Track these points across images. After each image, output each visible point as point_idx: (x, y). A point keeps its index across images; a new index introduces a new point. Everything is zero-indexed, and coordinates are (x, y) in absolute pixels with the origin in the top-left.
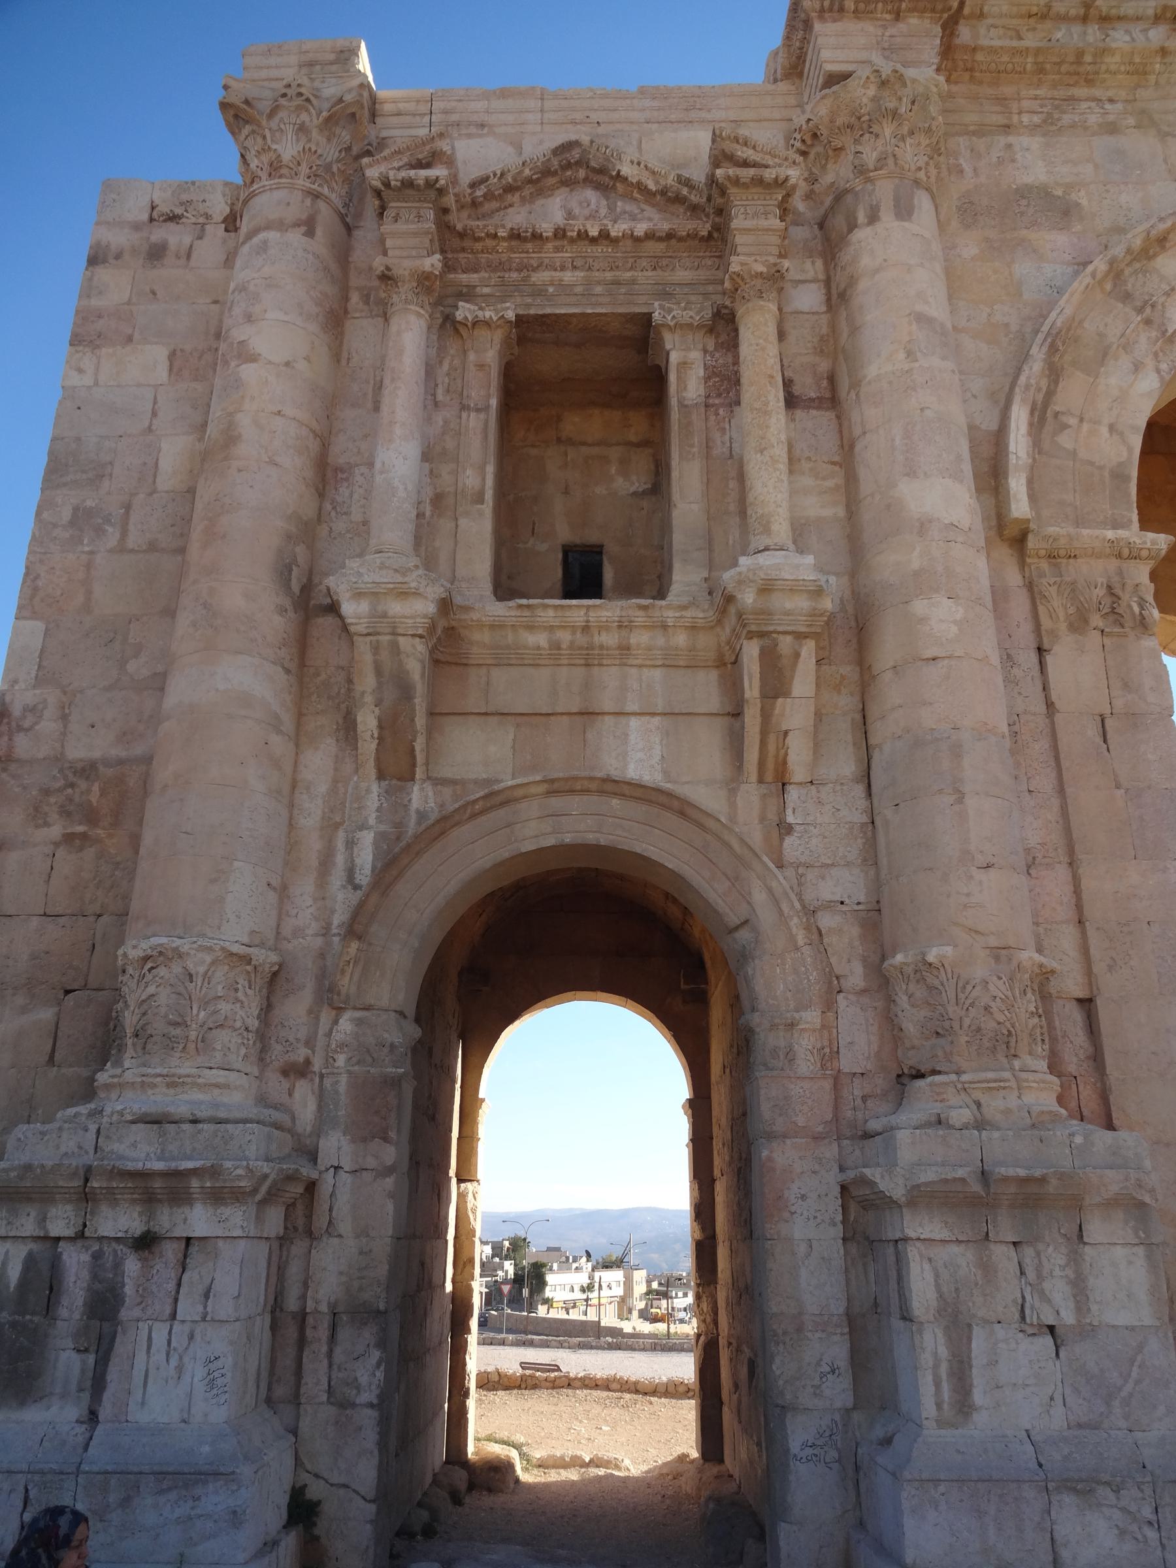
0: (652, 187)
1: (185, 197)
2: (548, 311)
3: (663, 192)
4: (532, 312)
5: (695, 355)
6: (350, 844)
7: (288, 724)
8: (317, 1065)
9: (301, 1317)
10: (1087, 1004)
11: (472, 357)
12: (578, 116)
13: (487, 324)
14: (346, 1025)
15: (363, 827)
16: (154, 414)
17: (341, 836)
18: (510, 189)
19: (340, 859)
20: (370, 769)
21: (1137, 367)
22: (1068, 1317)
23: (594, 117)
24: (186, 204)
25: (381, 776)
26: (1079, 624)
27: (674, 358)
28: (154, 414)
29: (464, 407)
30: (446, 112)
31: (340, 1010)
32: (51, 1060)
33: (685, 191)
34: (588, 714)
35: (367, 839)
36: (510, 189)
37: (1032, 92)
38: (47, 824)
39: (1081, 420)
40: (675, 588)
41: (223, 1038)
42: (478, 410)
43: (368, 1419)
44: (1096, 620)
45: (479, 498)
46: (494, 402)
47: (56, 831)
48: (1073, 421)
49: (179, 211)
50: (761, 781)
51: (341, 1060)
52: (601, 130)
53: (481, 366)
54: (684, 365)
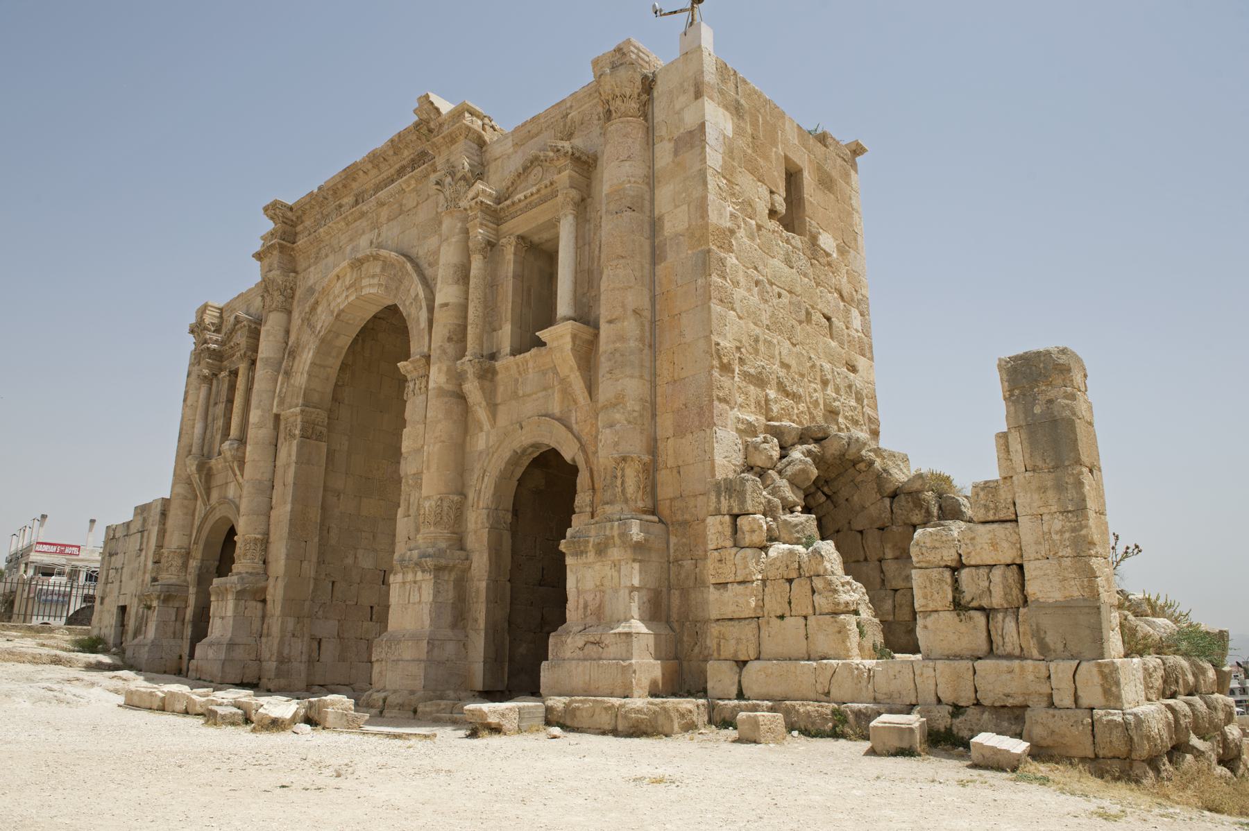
7: (190, 496)
18: (231, 333)
21: (309, 349)
34: (227, 483)
41: (173, 569)
43: (189, 641)
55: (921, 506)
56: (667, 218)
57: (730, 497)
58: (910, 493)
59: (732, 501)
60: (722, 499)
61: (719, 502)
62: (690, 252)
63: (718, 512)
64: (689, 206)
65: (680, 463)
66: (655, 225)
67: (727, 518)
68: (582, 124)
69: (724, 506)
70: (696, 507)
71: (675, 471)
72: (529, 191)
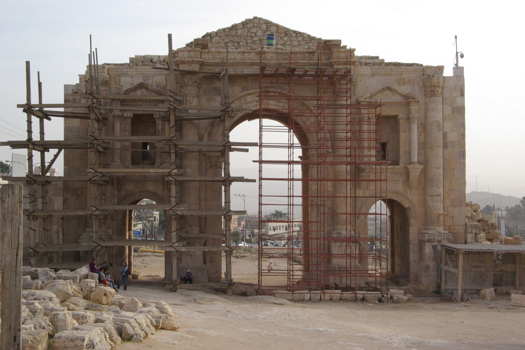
0: (154, 90)
1: (78, 88)
2: (138, 113)
3: (155, 91)
4: (136, 113)
5: (160, 122)
6: (114, 199)
8: (112, 227)
9: (112, 255)
10: (206, 218)
11: (127, 122)
12: (142, 73)
13: (129, 117)
14: (115, 222)
15: (115, 196)
16: (79, 132)
17: (112, 198)
19: (112, 201)
20: (116, 189)
22: (192, 254)
23: (145, 73)
24: (78, 90)
25: (117, 190)
26: (211, 168)
27: (157, 122)
28: (79, 132)
29: (126, 131)
30: (120, 71)
31: (114, 221)
32: (79, 227)
33: (159, 92)
35: (116, 198)
36: (131, 90)
37: (217, 68)
38: (73, 197)
39: (216, 135)
40: (156, 163)
42: (128, 131)
44: (213, 167)
45: (129, 147)
46: (130, 130)
47: (75, 198)
48: (214, 135)
49: (77, 91)
50: (167, 190)
51: (115, 226)
52: (146, 75)
53: (128, 124)
54: (159, 124)
55: (488, 225)
56: (448, 134)
57: (476, 229)
58: (485, 221)
59: (476, 230)
60: (473, 229)
61: (472, 230)
62: (458, 149)
63: (472, 233)
64: (458, 133)
65: (453, 216)
66: (445, 136)
67: (474, 235)
68: (410, 81)
69: (474, 231)
70: (459, 229)
71: (451, 217)
72: (387, 101)
